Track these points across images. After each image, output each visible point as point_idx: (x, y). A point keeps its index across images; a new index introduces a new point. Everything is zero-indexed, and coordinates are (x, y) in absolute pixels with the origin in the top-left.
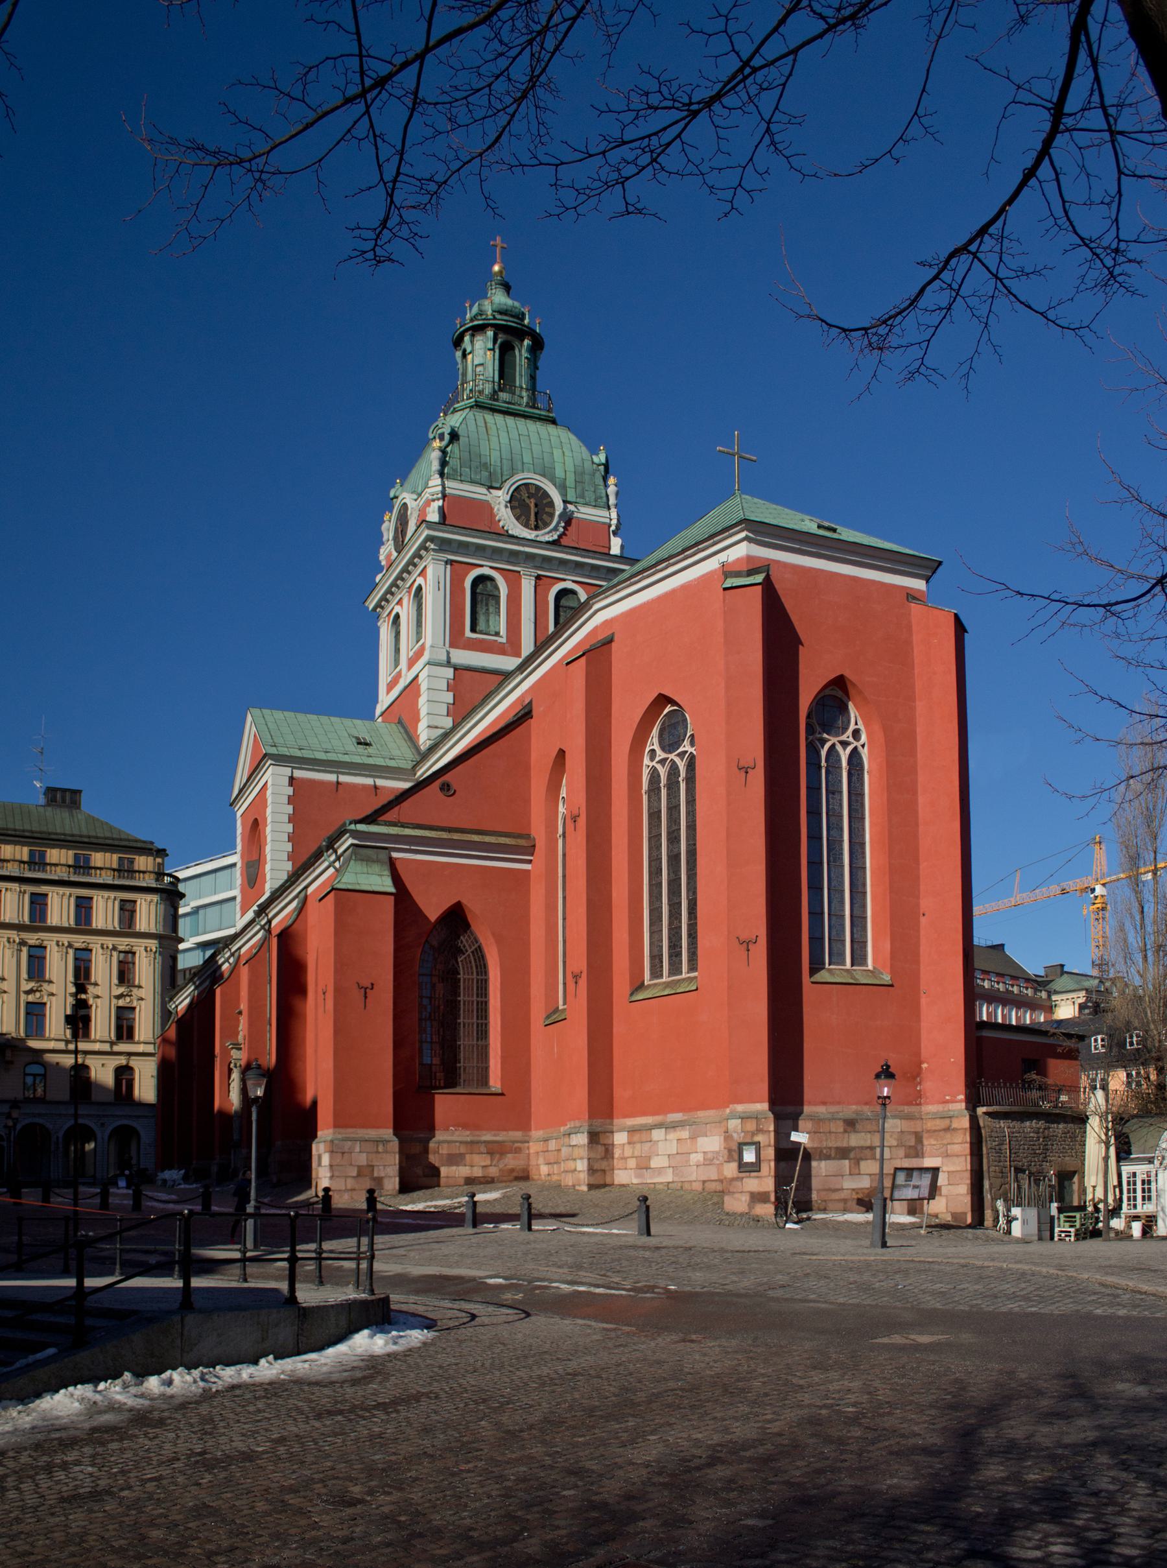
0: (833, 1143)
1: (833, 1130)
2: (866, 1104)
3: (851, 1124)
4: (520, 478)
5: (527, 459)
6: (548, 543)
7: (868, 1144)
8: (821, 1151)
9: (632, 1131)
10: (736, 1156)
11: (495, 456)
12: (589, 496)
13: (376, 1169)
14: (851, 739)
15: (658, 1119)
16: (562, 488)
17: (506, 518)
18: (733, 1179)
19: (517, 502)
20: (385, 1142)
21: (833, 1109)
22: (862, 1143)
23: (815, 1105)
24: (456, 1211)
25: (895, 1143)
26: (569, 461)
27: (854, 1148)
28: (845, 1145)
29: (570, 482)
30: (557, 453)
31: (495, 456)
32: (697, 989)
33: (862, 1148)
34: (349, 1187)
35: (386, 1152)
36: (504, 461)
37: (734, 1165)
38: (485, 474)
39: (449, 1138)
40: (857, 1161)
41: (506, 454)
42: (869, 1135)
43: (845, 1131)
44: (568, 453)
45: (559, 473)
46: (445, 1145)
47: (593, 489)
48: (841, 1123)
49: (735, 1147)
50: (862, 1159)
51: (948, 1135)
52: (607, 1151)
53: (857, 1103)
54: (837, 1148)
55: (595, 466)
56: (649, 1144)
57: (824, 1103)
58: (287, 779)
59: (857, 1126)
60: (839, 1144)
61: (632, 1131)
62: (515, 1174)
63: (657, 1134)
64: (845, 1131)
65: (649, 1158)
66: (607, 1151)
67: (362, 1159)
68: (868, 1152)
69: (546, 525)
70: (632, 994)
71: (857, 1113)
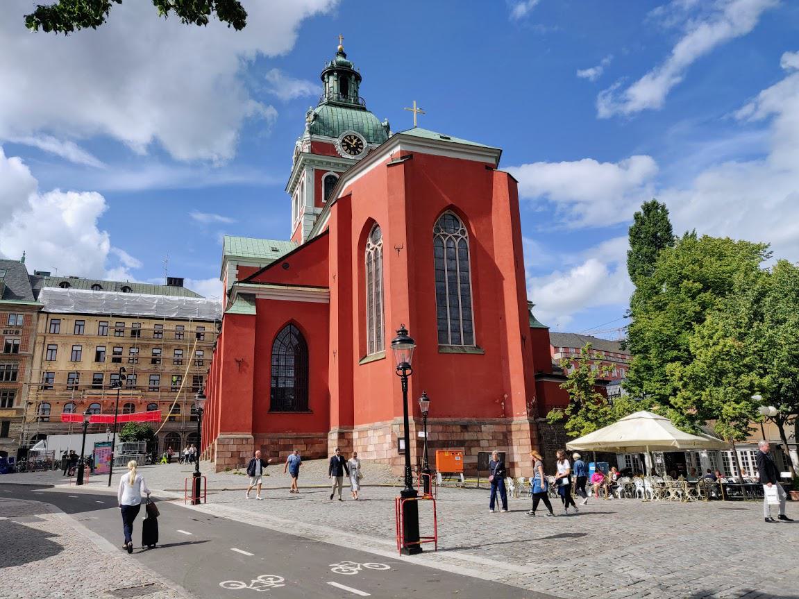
0: (455, 437)
1: (455, 430)
2: (474, 417)
3: (465, 428)
4: (347, 132)
5: (350, 123)
7: (475, 438)
9: (360, 432)
10: (397, 445)
11: (336, 124)
13: (241, 453)
15: (371, 424)
16: (367, 137)
18: (396, 458)
19: (346, 145)
20: (246, 439)
21: (454, 419)
22: (472, 438)
23: (444, 417)
24: (343, 468)
25: (491, 438)
27: (467, 441)
28: (462, 439)
31: (336, 124)
32: (385, 358)
33: (472, 440)
34: (226, 463)
35: (247, 444)
37: (396, 450)
39: (283, 436)
40: (470, 448)
43: (462, 432)
46: (282, 440)
48: (459, 426)
49: (396, 440)
50: (472, 447)
51: (519, 433)
52: (349, 442)
53: (470, 417)
54: (457, 441)
56: (367, 439)
57: (450, 416)
59: (470, 429)
60: (458, 439)
61: (360, 432)
62: (320, 455)
63: (370, 433)
64: (462, 432)
65: (367, 446)
66: (349, 442)
67: (234, 448)
68: (476, 443)
69: (359, 153)
70: (360, 361)
71: (469, 421)
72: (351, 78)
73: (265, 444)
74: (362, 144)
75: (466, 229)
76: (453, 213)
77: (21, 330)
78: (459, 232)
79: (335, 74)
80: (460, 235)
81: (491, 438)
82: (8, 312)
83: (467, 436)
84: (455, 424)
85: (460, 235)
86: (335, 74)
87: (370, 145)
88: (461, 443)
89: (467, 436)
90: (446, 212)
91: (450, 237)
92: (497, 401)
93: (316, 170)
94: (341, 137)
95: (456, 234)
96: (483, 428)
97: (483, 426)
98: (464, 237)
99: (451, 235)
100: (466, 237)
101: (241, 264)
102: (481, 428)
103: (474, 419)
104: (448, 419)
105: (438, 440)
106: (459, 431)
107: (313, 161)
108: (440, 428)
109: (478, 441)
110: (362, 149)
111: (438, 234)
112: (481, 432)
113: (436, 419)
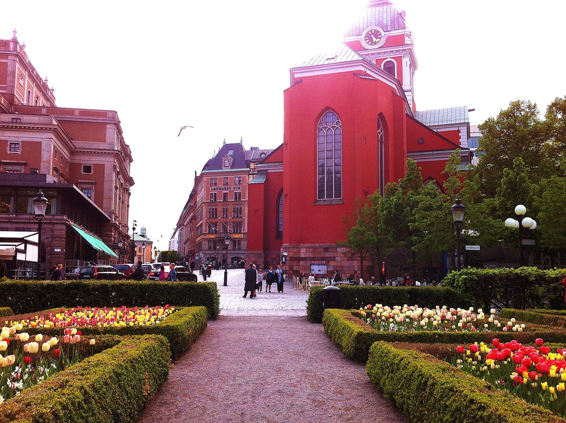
3: (326, 250)
6: (379, 48)
8: (315, 258)
12: (397, 26)
17: (364, 44)
26: (389, 17)
29: (389, 24)
30: (385, 15)
33: (330, 257)
41: (365, 22)
42: (333, 253)
43: (324, 252)
45: (385, 22)
55: (399, 15)
57: (318, 243)
59: (329, 250)
60: (321, 256)
64: (324, 252)
71: (329, 246)
73: (273, 257)
74: (380, 35)
75: (340, 121)
77: (241, 187)
80: (336, 125)
82: (234, 176)
83: (328, 255)
84: (320, 247)
85: (336, 125)
87: (387, 33)
88: (323, 259)
89: (328, 255)
94: (364, 34)
97: (338, 249)
103: (333, 244)
104: (318, 245)
105: (310, 257)
108: (311, 250)
109: (334, 258)
110: (380, 38)
113: (309, 245)
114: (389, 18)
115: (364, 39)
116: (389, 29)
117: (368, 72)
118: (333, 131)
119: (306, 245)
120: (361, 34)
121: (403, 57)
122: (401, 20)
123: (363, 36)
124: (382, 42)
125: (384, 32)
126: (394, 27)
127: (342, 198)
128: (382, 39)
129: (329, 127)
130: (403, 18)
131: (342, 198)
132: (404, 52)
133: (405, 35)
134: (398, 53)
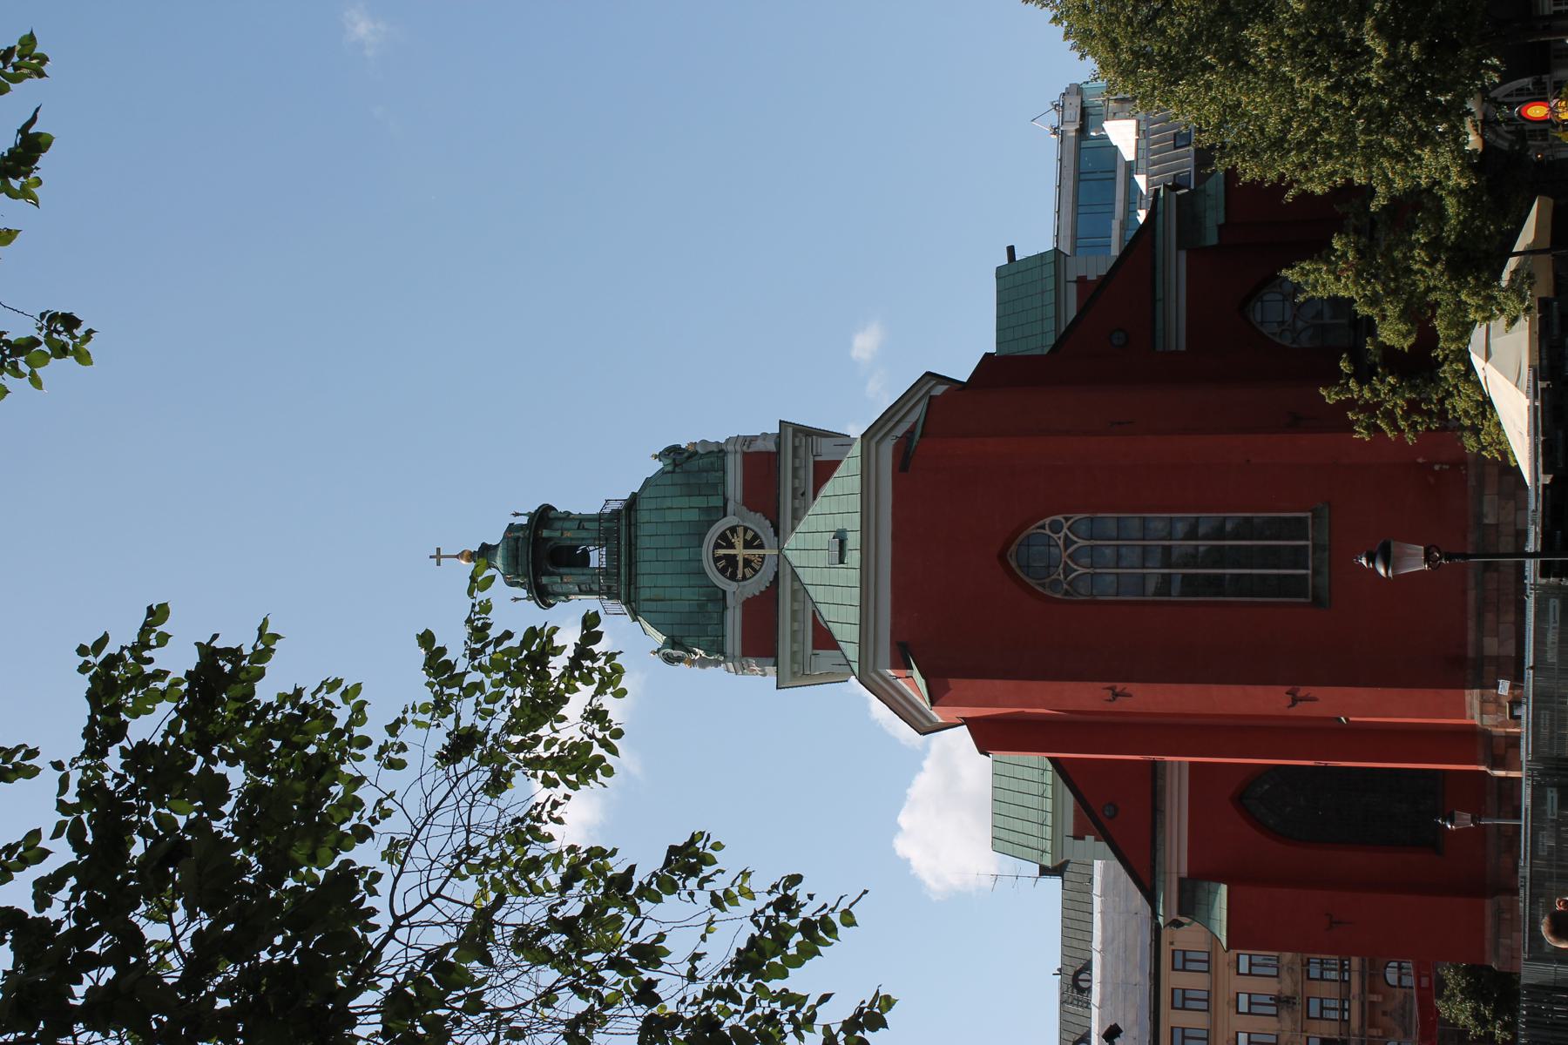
5: (683, 554)
12: (713, 477)
14: (1062, 534)
17: (755, 585)
21: (1471, 582)
25: (1512, 503)
29: (700, 502)
30: (672, 516)
36: (692, 583)
38: (710, 606)
44: (668, 503)
45: (694, 516)
47: (705, 474)
55: (677, 470)
58: (1076, 841)
72: (549, 539)
75: (1047, 521)
76: (1013, 548)
78: (1055, 536)
79: (544, 580)
81: (1512, 503)
85: (1062, 534)
86: (544, 580)
90: (1013, 564)
91: (1070, 556)
92: (1432, 480)
93: (814, 647)
95: (1061, 543)
96: (1490, 520)
97: (1486, 521)
98: (1066, 526)
99: (1064, 555)
100: (1067, 519)
101: (1070, 830)
102: (1492, 525)
104: (1472, 596)
106: (1495, 575)
107: (794, 654)
108: (1490, 617)
111: (1065, 586)
112: (1497, 526)
113: (1471, 624)
114: (684, 502)
115: (741, 583)
116: (716, 501)
117: (900, 431)
118: (1081, 543)
119: (1471, 637)
120: (721, 595)
121: (818, 459)
122: (695, 464)
123: (730, 587)
124: (758, 523)
125: (725, 515)
126: (715, 486)
127: (1309, 514)
128: (746, 524)
129: (1064, 555)
130: (689, 457)
131: (1309, 514)
132: (802, 452)
133: (745, 448)
134: (802, 473)
